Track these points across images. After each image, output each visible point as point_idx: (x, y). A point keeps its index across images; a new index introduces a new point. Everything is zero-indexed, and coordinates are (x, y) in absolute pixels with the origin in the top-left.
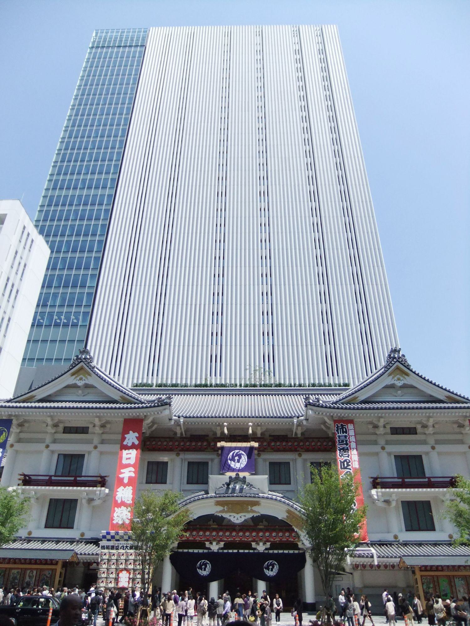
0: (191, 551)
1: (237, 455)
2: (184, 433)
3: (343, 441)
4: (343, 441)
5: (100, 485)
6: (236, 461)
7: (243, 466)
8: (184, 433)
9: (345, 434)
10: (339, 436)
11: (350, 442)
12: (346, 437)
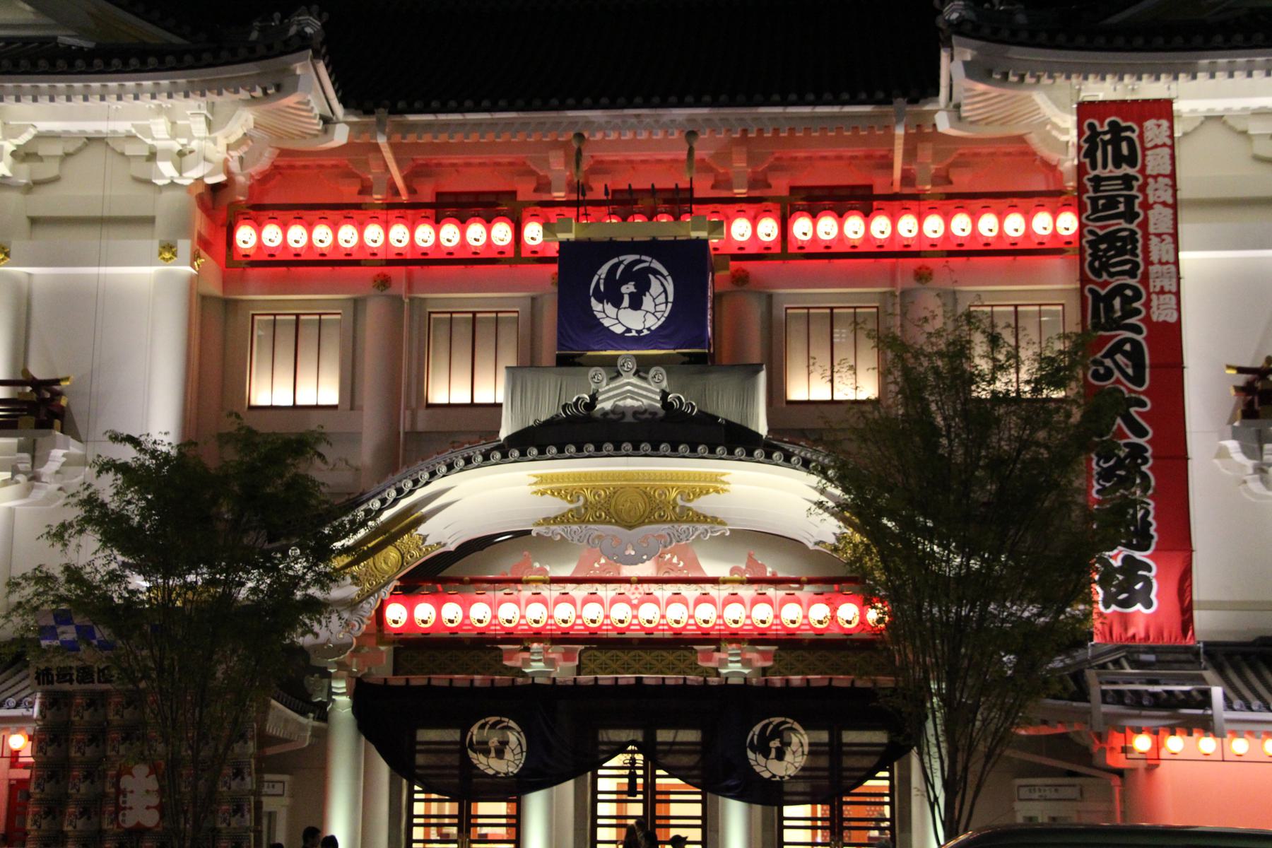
0: (440, 680)
1: (628, 275)
2: (400, 183)
3: (1112, 202)
4: (1112, 202)
5: (32, 420)
6: (626, 302)
7: (653, 323)
8: (400, 183)
9: (1126, 169)
10: (1097, 181)
11: (1147, 206)
12: (1127, 180)
